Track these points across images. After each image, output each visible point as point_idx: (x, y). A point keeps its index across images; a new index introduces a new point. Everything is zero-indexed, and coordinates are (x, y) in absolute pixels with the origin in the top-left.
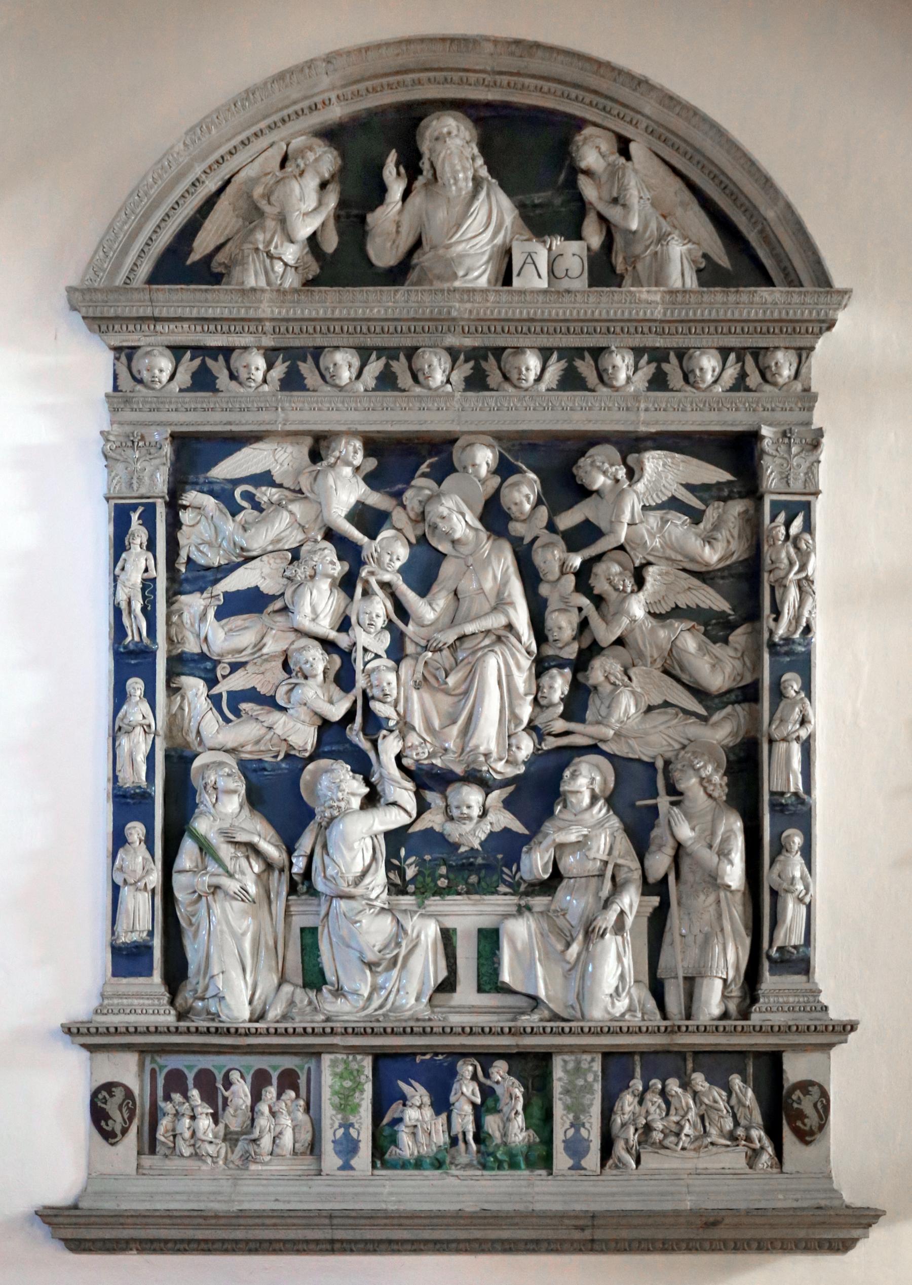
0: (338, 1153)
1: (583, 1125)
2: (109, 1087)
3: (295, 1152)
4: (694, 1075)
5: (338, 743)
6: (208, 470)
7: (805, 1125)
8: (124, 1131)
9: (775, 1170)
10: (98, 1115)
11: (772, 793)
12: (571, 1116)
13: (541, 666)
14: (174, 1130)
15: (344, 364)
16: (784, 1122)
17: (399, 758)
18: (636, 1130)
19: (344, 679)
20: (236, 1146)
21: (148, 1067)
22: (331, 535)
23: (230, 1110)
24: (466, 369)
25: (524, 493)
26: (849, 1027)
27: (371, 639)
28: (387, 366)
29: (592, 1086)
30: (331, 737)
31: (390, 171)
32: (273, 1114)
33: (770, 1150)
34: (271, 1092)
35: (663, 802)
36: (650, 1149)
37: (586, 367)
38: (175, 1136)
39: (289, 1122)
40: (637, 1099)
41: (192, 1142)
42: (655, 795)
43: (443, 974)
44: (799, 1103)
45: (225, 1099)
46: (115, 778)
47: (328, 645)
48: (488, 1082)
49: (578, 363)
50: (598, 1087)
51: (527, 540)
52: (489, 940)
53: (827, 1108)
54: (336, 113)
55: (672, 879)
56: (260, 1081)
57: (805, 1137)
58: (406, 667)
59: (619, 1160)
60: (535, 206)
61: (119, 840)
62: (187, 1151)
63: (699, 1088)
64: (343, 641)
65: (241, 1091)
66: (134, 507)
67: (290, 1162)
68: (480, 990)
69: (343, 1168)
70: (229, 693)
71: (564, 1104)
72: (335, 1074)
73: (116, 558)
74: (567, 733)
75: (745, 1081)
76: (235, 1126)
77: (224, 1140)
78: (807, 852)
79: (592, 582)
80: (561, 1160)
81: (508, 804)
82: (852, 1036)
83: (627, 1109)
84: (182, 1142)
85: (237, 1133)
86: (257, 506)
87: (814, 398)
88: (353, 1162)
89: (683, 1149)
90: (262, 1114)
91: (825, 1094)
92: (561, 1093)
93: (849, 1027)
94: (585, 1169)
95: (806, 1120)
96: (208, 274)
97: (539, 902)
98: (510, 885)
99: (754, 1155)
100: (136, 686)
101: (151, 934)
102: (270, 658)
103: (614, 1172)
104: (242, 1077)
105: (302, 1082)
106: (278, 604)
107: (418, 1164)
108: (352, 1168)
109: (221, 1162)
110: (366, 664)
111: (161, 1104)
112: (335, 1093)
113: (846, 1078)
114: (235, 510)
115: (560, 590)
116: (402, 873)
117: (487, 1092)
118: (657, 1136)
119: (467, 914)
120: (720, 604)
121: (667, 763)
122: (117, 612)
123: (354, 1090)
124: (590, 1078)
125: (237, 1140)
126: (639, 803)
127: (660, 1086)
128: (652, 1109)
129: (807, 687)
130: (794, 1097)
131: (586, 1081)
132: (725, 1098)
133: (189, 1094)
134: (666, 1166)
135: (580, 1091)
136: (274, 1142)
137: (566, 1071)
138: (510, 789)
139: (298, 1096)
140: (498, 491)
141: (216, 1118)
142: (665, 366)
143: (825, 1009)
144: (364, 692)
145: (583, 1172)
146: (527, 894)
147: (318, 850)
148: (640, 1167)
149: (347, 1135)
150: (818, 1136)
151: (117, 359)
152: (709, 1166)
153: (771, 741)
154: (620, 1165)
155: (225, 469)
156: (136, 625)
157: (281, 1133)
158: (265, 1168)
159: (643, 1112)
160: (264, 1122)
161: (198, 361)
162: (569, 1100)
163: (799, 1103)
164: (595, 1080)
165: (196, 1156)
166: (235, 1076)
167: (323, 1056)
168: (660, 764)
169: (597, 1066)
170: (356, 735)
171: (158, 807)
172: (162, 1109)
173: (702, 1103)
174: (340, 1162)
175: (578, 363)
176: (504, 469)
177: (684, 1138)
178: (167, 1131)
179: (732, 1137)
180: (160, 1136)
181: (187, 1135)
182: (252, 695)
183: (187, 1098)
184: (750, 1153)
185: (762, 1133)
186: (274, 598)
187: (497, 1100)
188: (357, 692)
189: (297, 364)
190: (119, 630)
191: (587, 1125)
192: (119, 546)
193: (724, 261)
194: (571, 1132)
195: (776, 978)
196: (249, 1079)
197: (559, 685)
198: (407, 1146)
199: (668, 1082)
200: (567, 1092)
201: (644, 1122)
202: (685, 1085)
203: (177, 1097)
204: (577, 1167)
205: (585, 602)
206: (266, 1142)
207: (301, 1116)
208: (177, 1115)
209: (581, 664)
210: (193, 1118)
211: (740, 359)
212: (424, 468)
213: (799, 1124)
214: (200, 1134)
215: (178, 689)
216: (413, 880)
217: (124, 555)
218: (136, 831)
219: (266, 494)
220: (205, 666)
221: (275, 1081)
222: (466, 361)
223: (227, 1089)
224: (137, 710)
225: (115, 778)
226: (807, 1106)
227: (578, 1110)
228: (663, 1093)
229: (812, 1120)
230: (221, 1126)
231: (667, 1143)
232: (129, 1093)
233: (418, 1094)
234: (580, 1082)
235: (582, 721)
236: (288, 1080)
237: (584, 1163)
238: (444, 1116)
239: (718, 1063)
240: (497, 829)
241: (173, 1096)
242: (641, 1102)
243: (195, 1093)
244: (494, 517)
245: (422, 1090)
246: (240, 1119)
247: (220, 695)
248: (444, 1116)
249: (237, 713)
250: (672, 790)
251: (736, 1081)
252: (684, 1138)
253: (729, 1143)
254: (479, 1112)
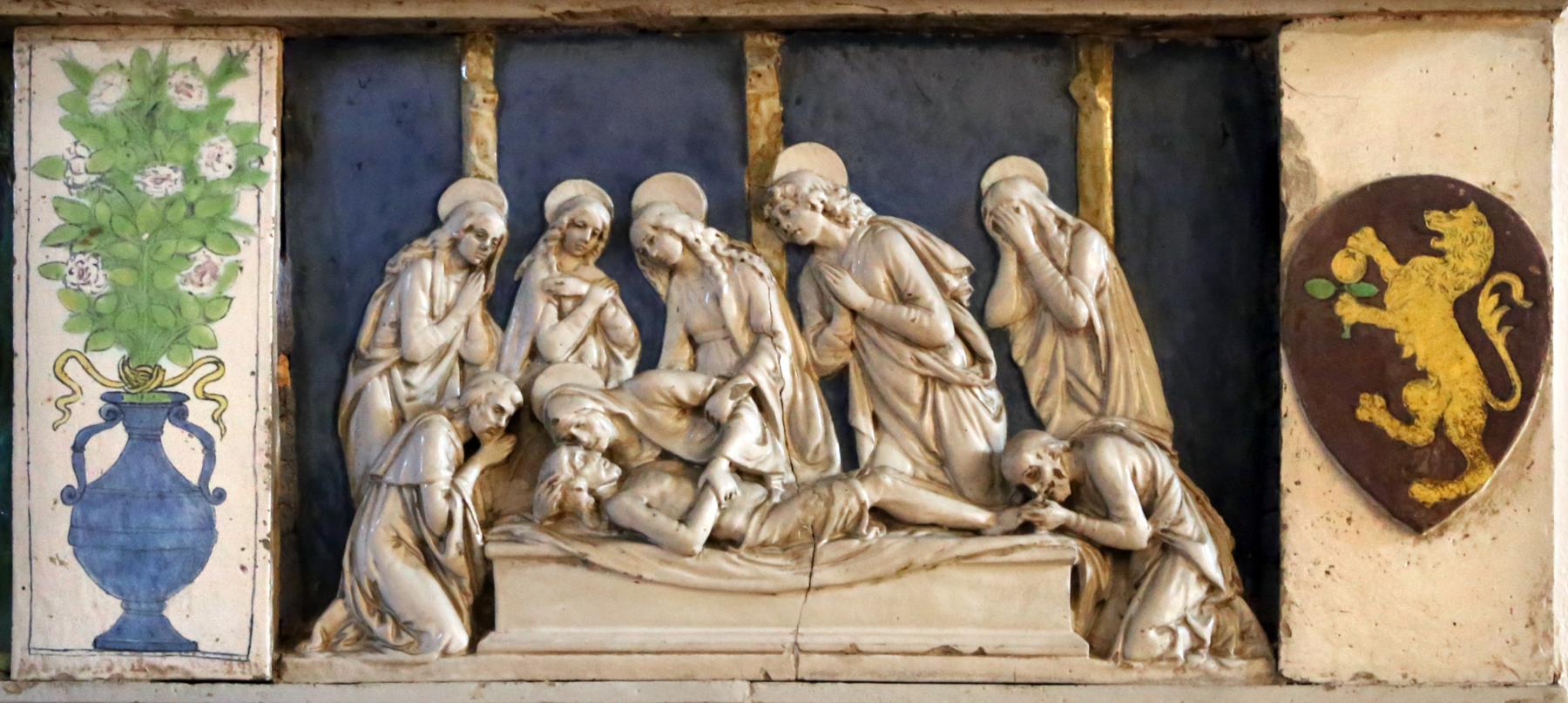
1: (177, 409)
4: (790, 160)
7: (1407, 418)
9: (1237, 666)
12: (109, 361)
16: (1289, 402)
18: (472, 446)
29: (225, 203)
33: (1209, 556)
36: (546, 544)
40: (478, 288)
44: (1376, 301)
50: (259, 207)
53: (1531, 328)
57: (1405, 485)
59: (378, 600)
63: (814, 226)
71: (70, 294)
83: (425, 336)
89: (719, 540)
91: (1518, 252)
92: (46, 241)
94: (191, 648)
95: (1413, 394)
99: (1115, 586)
103: (350, 665)
118: (580, 474)
127: (600, 214)
128: (562, 337)
130: (1344, 267)
131: (191, 174)
132: (960, 283)
134: (632, 634)
135: (163, 226)
137: (80, 121)
145: (179, 663)
148: (485, 643)
152: (867, 637)
154: (386, 631)
159: (516, 354)
162: (99, 281)
163: (1376, 301)
164: (240, 172)
169: (255, 101)
173: (830, 302)
177: (725, 482)
179: (1004, 488)
184: (1095, 571)
185: (1167, 469)
191: (199, 412)
194: (110, 446)
199: (642, 195)
201: (511, 398)
202: (741, 210)
213: (1371, 409)
227: (141, 323)
228: (622, 254)
229: (1450, 389)
231: (632, 507)
234: (161, 183)
242: (500, 306)
251: (1019, 189)
252: (725, 482)
253: (981, 516)
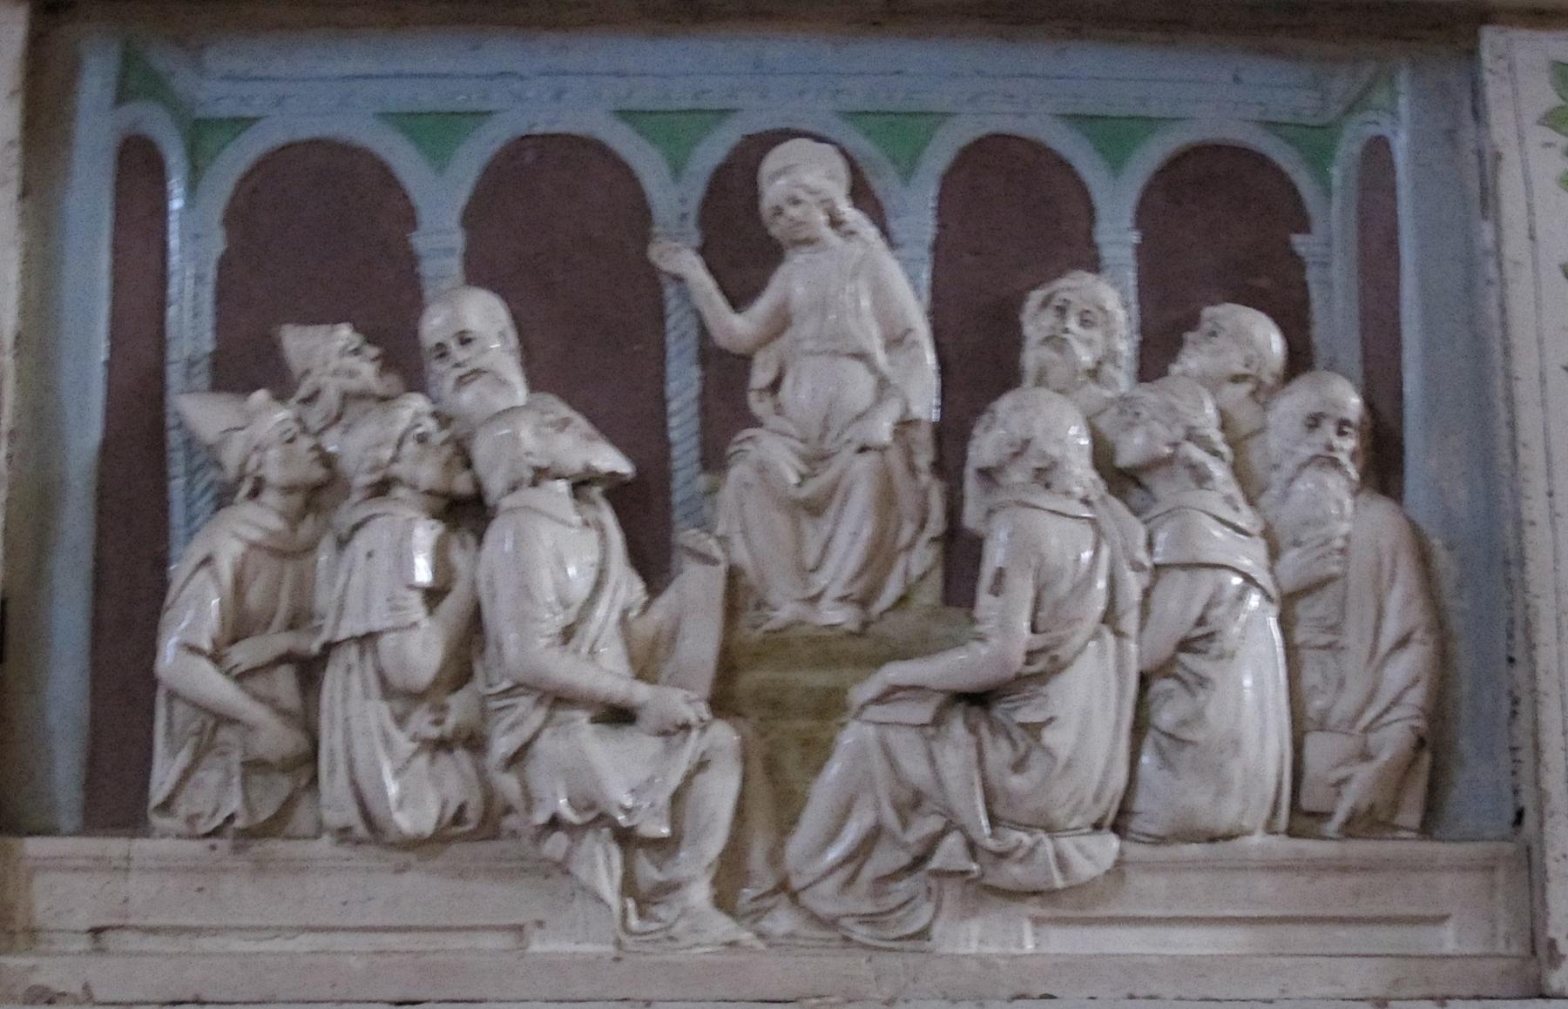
3: (1302, 818)
14: (299, 619)
20: (817, 752)
21: (95, 127)
23: (770, 452)
32: (1123, 480)
34: (1092, 315)
38: (310, 670)
39: (1251, 557)
41: (459, 708)
45: (726, 372)
56: (999, 236)
62: (415, 797)
65: (856, 307)
67: (1267, 892)
76: (818, 581)
77: (722, 704)
84: (378, 712)
85: (829, 650)
90: (1045, 476)
104: (861, 193)
105: (1328, 253)
109: (700, 894)
111: (200, 413)
125: (831, 707)
133: (434, 326)
136: (1140, 727)
139: (1299, 361)
141: (645, 520)
157: (1198, 639)
158: (1065, 942)
160: (1056, 539)
165: (480, 827)
166: (804, 179)
167: (1491, 39)
172: (205, 455)
178: (239, 627)
180: (186, 650)
181: (423, 649)
183: (405, 361)
196: (918, 210)
203: (328, 352)
206: (1086, 708)
207: (1336, 502)
208: (319, 494)
210: (464, 512)
214: (527, 645)
221: (1118, 235)
223: (739, 300)
230: (697, 587)
236: (1224, 234)
241: (298, 342)
243: (475, 321)
246: (849, 536)
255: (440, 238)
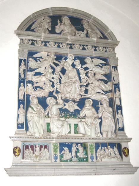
0: (54, 159)
2: (16, 147)
5: (52, 95)
6: (33, 55)
8: (19, 155)
10: (14, 152)
11: (116, 105)
13: (81, 86)
15: (52, 43)
17: (61, 97)
19: (53, 86)
22: (50, 66)
24: (70, 46)
25: (77, 62)
26: (131, 139)
27: (56, 80)
28: (59, 45)
30: (51, 94)
31: (58, 21)
34: (43, 149)
35: (100, 106)
37: (86, 47)
42: (99, 105)
43: (69, 131)
45: (35, 150)
46: (18, 98)
47: (51, 81)
48: (78, 148)
49: (85, 47)
50: (95, 148)
51: (78, 69)
52: (76, 125)
54: (51, 14)
55: (102, 116)
58: (62, 85)
60: (77, 28)
61: (19, 107)
64: (53, 80)
66: (23, 59)
68: (75, 133)
69: (55, 161)
70: (36, 87)
72: (53, 146)
73: (20, 66)
74: (85, 96)
75: (116, 147)
78: (122, 113)
79: (88, 74)
80: (90, 160)
81: (77, 105)
82: (131, 140)
85: (37, 156)
86: (40, 61)
87: (116, 54)
88: (57, 160)
91: (128, 149)
93: (131, 139)
96: (33, 30)
97: (83, 120)
98: (78, 117)
100: (22, 84)
101: (24, 122)
102: (43, 81)
105: (48, 147)
106: (43, 75)
107: (67, 161)
108: (57, 161)
110: (56, 84)
112: (54, 149)
113: (131, 146)
114: (37, 61)
115: (83, 76)
116: (62, 115)
117: (77, 149)
119: (73, 121)
120: (106, 79)
121: (100, 101)
122: (20, 74)
123: (57, 148)
124: (93, 147)
126: (97, 106)
129: (119, 91)
138: (77, 103)
140: (74, 62)
142: (95, 48)
143: (127, 136)
144: (56, 88)
146: (81, 119)
147: (50, 111)
149: (56, 156)
150: (128, 156)
151: (20, 40)
153: (115, 98)
155: (35, 56)
156: (22, 75)
161: (32, 41)
162: (90, 150)
166: (37, 146)
168: (99, 101)
170: (54, 94)
171: (24, 103)
174: (55, 160)
175: (85, 47)
176: (75, 59)
182: (39, 87)
186: (42, 74)
187: (79, 150)
188: (55, 87)
189: (45, 43)
190: (20, 76)
192: (20, 65)
193: (103, 37)
194: (91, 155)
195: (119, 132)
197: (84, 89)
198: (65, 158)
200: (90, 149)
202: (107, 148)
204: (92, 161)
205: (87, 77)
209: (87, 86)
211: (106, 48)
212: (63, 58)
215: (27, 86)
216: (64, 116)
217: (21, 66)
218: (22, 106)
219: (41, 59)
220: (31, 82)
222: (70, 45)
224: (22, 87)
225: (18, 98)
226: (126, 151)
229: (127, 153)
230: (35, 154)
232: (20, 149)
233: (66, 149)
234: (92, 147)
235: (87, 94)
237: (93, 160)
238: (71, 153)
239: (112, 145)
240: (76, 109)
243: (30, 149)
244: (73, 65)
245: (67, 149)
247: (34, 87)
248: (71, 153)
249: (37, 90)
250: (101, 104)
251: (114, 147)
254: (76, 152)
255: (29, 147)
